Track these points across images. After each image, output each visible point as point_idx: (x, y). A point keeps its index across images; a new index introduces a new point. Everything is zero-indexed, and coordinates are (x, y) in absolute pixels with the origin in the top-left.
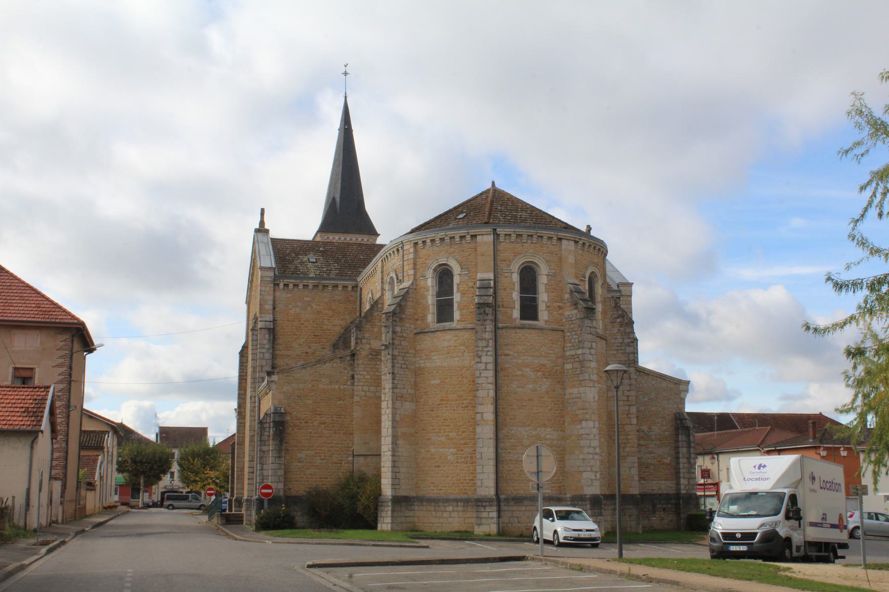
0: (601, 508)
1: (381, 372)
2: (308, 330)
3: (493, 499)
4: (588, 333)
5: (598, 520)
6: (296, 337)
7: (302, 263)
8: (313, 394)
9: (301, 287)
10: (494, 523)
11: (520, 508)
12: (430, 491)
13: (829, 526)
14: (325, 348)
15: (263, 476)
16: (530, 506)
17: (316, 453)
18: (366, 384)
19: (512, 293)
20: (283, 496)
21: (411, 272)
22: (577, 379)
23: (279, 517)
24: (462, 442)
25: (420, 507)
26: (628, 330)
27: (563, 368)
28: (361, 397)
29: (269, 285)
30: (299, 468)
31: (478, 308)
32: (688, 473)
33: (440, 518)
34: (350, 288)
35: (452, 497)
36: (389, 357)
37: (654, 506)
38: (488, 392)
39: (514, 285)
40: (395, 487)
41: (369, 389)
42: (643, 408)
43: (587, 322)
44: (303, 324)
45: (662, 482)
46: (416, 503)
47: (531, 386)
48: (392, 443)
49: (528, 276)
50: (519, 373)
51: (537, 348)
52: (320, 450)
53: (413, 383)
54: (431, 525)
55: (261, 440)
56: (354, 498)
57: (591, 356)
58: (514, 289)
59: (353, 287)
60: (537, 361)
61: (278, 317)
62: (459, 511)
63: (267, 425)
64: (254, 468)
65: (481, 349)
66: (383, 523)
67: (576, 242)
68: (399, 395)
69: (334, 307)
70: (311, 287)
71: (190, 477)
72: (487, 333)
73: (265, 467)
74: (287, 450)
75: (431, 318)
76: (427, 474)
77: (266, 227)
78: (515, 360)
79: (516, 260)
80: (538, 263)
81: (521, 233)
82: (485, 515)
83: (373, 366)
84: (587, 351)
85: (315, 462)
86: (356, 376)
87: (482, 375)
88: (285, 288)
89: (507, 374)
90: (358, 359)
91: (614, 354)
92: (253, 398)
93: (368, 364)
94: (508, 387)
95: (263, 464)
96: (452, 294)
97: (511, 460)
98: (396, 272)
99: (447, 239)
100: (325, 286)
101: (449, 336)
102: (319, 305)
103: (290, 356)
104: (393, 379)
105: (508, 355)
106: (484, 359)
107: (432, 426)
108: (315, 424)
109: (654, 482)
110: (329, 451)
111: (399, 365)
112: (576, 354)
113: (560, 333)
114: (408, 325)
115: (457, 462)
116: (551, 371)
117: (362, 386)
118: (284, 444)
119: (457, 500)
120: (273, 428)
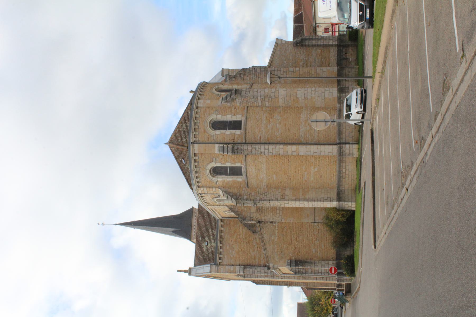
0: (345, 88)
1: (269, 207)
2: (245, 246)
3: (339, 146)
4: (249, 93)
5: (351, 89)
6: (249, 254)
7: (208, 250)
8: (280, 244)
9: (221, 250)
10: (352, 146)
11: (344, 132)
12: (334, 181)
14: (255, 237)
15: (325, 272)
17: (312, 243)
18: (275, 215)
19: (227, 134)
20: (336, 262)
21: (214, 189)
22: (274, 100)
23: (347, 263)
24: (308, 163)
25: (343, 186)
26: (248, 71)
27: (268, 107)
28: (282, 218)
29: (220, 268)
30: (321, 252)
31: (234, 153)
32: (326, 40)
33: (349, 176)
34: (222, 223)
35: (337, 169)
36: (260, 202)
37: (344, 59)
38: (281, 148)
39: (222, 133)
40: (332, 199)
41: (278, 214)
42: (291, 64)
43: (243, 93)
44: (242, 249)
45: (331, 55)
46: (341, 188)
47: (278, 125)
48: (308, 201)
49: (217, 125)
50: (270, 131)
51: (257, 121)
52: (311, 241)
53: (275, 189)
54: (353, 180)
55: (306, 273)
56: (338, 222)
57: (262, 92)
58: (224, 133)
59: (221, 222)
60: (264, 121)
61: (238, 263)
62: (346, 165)
63: (297, 271)
64: (320, 277)
65: (257, 152)
66: (351, 206)
67: (199, 99)
68: (281, 197)
69: (233, 232)
70: (221, 245)
71: (325, 312)
72: (248, 148)
73: (320, 271)
74: (311, 259)
75: (239, 179)
76: (325, 182)
77: (188, 269)
78: (264, 133)
79: (208, 132)
80: (210, 120)
81: (194, 129)
82: (347, 151)
83: (266, 211)
84: (259, 94)
85: (318, 243)
86: (271, 221)
87: (271, 151)
88: (221, 259)
89: (271, 138)
90: (262, 220)
91: (261, 79)
92: (282, 277)
93: (264, 214)
94: (278, 137)
95: (318, 272)
96: (227, 167)
97: (318, 137)
98: (214, 198)
99: (196, 169)
100: (221, 237)
101: (249, 169)
102: (231, 240)
103: (259, 257)
104: (273, 200)
105: (260, 137)
106: (262, 150)
107: (299, 179)
108: (296, 244)
109: (331, 58)
110: (312, 236)
111: (265, 197)
112: (261, 100)
113: (249, 108)
114: (243, 192)
115: (319, 166)
116: (270, 114)
117: (276, 217)
118: (307, 261)
119: (340, 166)
120: (298, 267)
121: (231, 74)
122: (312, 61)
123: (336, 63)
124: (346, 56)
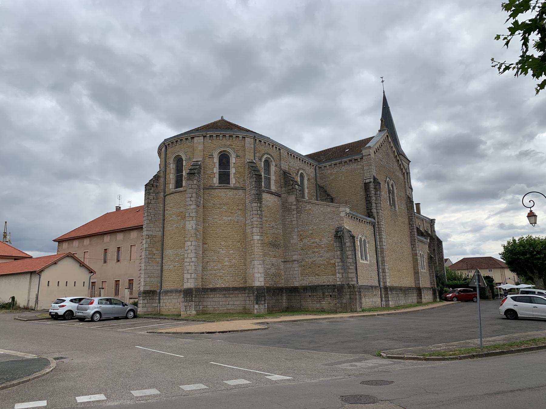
13: (48, 316)
16: (170, 296)
37: (324, 293)
42: (316, 227)
45: (329, 276)
49: (224, 160)
50: (171, 219)
57: (191, 202)
60: (179, 211)
109: (325, 277)
121: (364, 159)
122: (320, 253)
123: (319, 284)
124: (327, 296)
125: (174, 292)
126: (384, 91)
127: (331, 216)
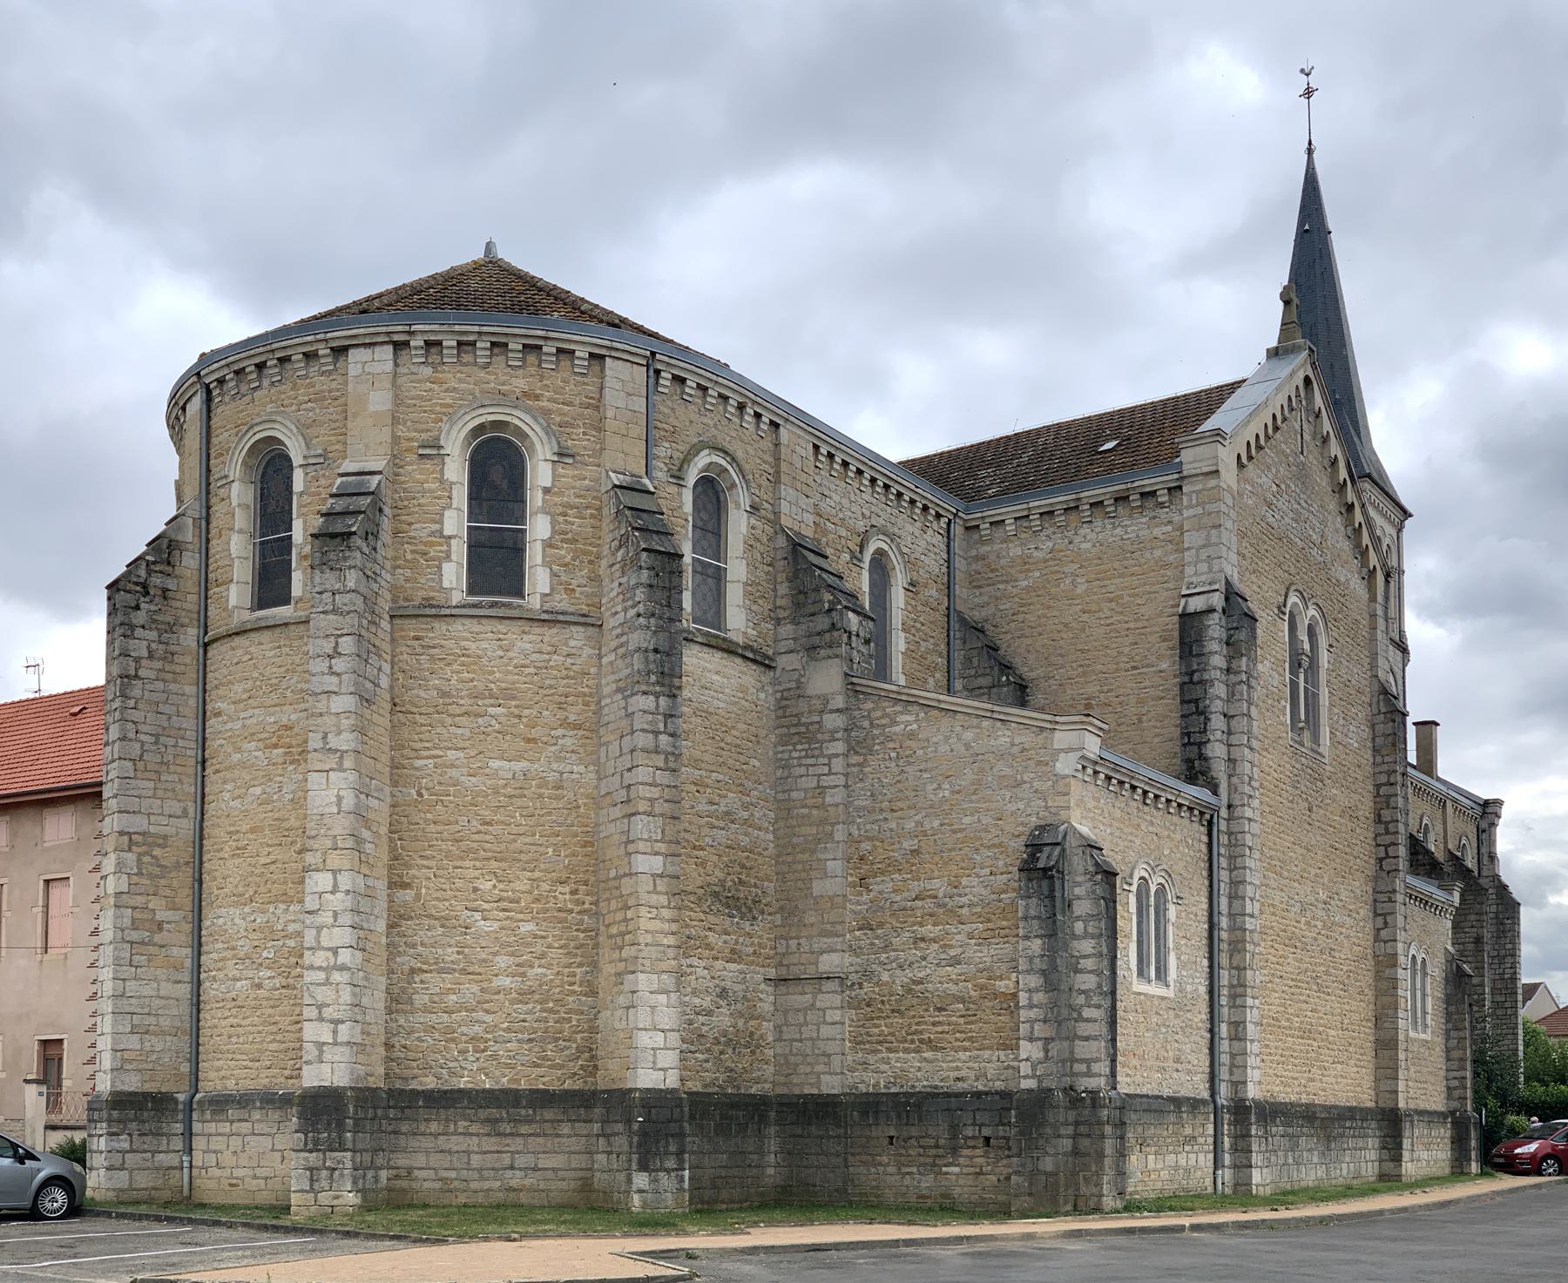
4: (323, 612)
16: (239, 1120)
37: (954, 1130)
42: (936, 823)
45: (986, 1054)
47: (258, 790)
50: (236, 757)
57: (335, 679)
60: (272, 720)
109: (962, 1055)
122: (951, 947)
123: (936, 1087)
125: (258, 1104)
126: (1310, 143)
127: (1008, 771)
